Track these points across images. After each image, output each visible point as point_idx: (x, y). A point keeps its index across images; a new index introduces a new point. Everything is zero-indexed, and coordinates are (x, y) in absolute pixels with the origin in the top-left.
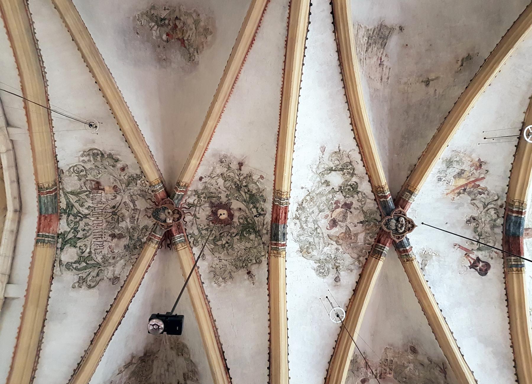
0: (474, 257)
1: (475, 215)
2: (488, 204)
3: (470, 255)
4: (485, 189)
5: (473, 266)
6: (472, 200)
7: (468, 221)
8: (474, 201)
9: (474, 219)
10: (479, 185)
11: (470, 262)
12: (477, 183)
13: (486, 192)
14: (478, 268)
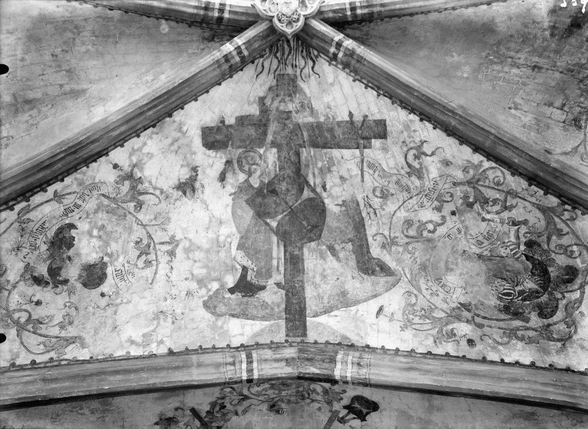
0: (344, 412)
1: (265, 407)
2: (242, 395)
3: (341, 415)
4: (213, 405)
5: (362, 417)
6: (236, 414)
7: (278, 412)
8: (240, 412)
9: (272, 406)
10: (208, 412)
11: (354, 418)
12: (203, 415)
13: (220, 401)
14: (365, 411)
